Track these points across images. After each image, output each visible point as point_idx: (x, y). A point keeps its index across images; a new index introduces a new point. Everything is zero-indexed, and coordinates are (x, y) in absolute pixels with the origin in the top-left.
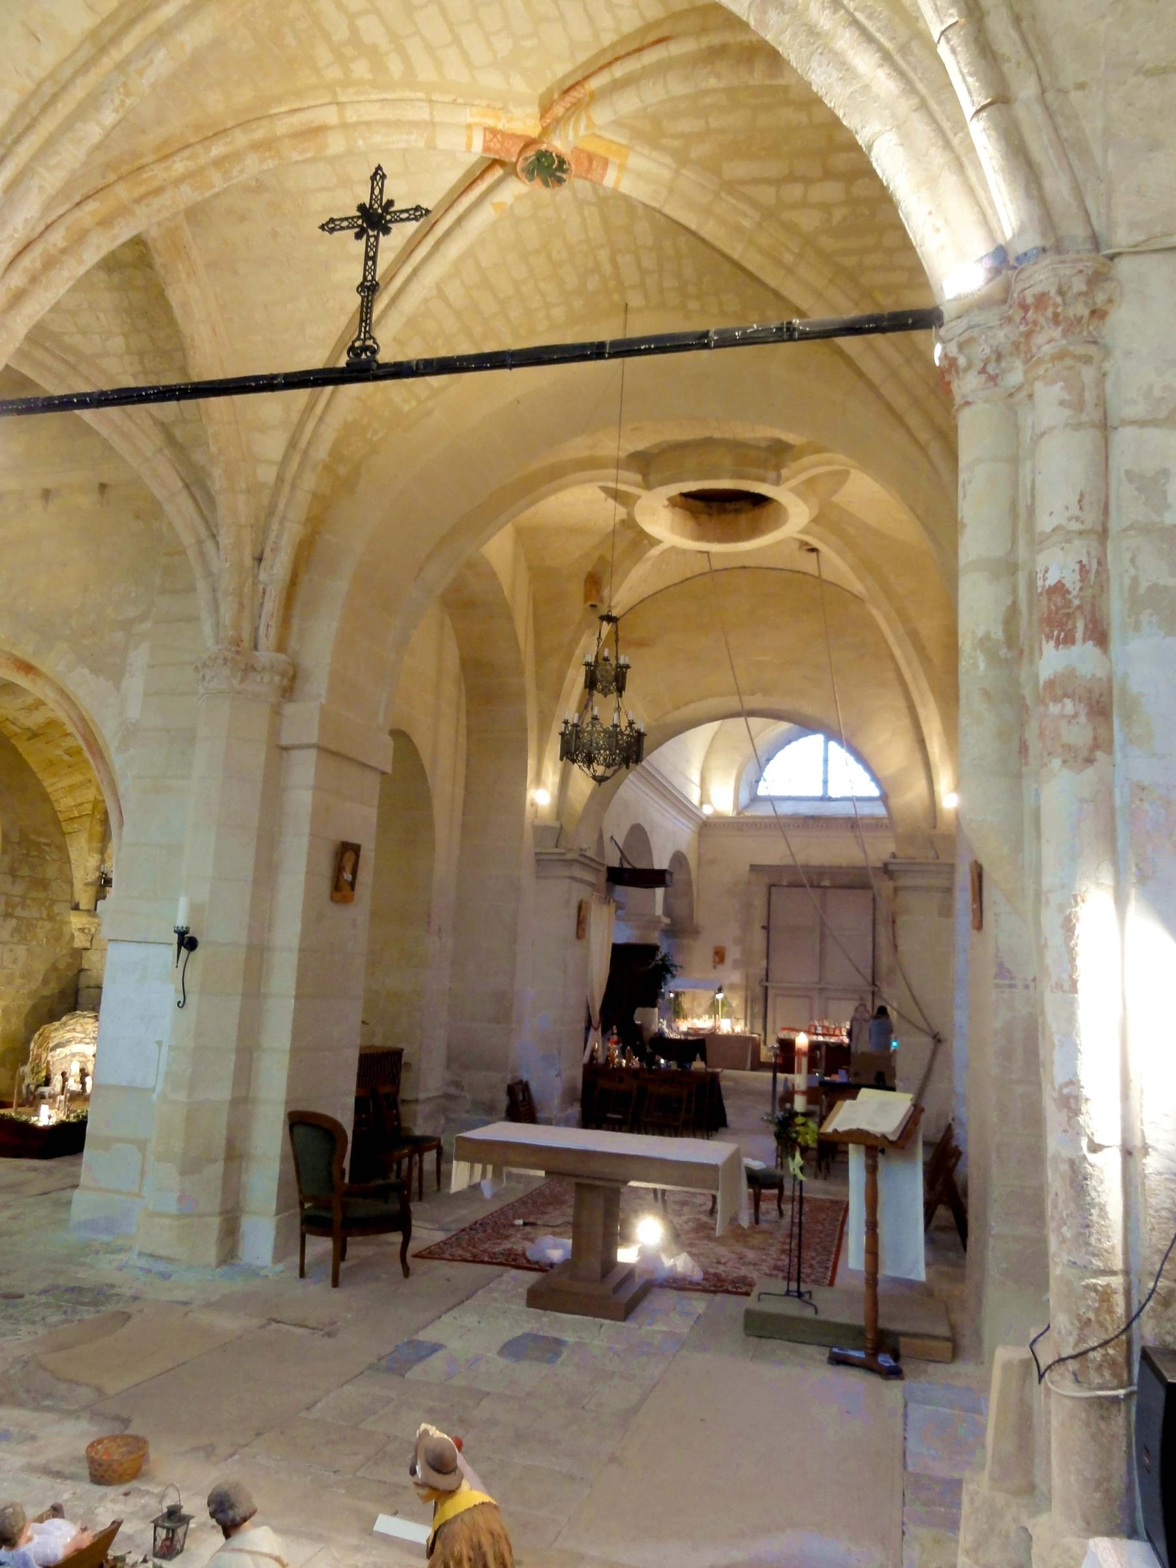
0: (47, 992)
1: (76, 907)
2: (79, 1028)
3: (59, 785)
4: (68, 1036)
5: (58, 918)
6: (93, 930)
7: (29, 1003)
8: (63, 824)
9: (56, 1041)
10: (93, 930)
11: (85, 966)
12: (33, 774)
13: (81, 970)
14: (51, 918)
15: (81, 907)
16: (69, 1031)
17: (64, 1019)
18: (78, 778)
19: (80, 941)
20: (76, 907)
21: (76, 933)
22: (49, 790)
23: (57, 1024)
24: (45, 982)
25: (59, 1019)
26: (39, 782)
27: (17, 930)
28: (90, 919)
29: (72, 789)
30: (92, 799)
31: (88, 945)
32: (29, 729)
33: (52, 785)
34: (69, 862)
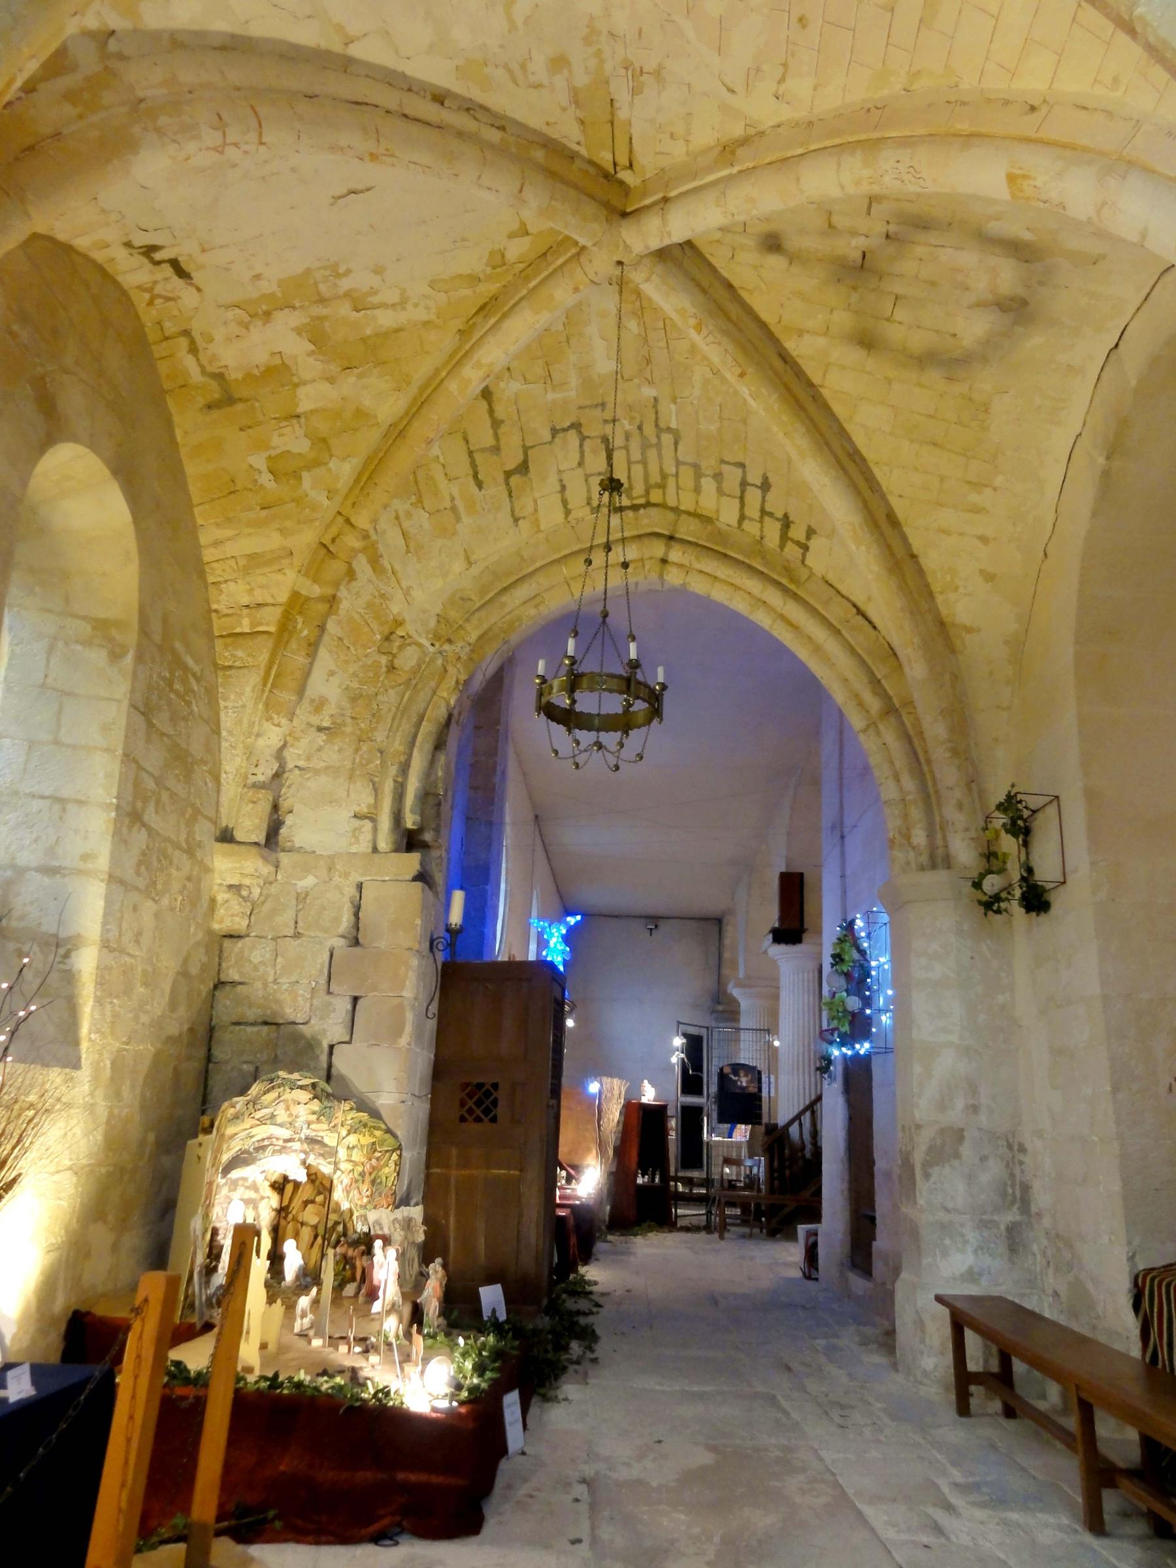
0: (173, 1029)
1: (226, 837)
2: (282, 1115)
3: (230, 549)
4: (261, 1132)
5: (199, 855)
6: (256, 892)
7: (146, 1049)
8: (219, 644)
9: (235, 1147)
10: (256, 892)
11: (233, 975)
12: (190, 506)
13: (219, 985)
14: (190, 852)
15: (239, 836)
16: (262, 1122)
17: (255, 1089)
18: (270, 541)
19: (229, 915)
20: (226, 837)
21: (221, 897)
22: (209, 555)
23: (240, 1101)
24: (173, 1005)
25: (243, 1091)
26: (194, 530)
27: (144, 861)
28: (260, 863)
29: (255, 561)
30: (283, 597)
31: (240, 924)
32: (219, 377)
33: (217, 543)
34: (217, 731)
